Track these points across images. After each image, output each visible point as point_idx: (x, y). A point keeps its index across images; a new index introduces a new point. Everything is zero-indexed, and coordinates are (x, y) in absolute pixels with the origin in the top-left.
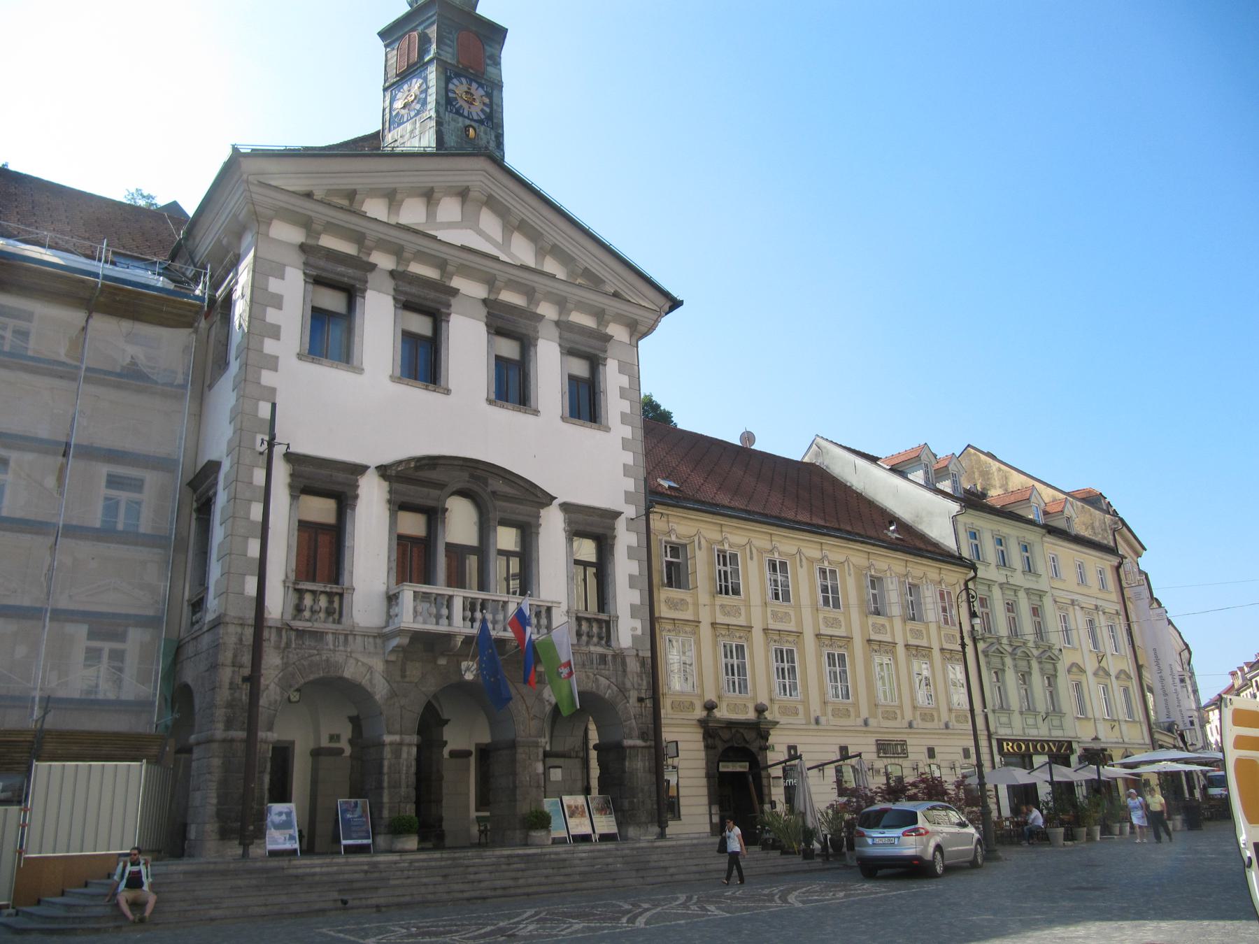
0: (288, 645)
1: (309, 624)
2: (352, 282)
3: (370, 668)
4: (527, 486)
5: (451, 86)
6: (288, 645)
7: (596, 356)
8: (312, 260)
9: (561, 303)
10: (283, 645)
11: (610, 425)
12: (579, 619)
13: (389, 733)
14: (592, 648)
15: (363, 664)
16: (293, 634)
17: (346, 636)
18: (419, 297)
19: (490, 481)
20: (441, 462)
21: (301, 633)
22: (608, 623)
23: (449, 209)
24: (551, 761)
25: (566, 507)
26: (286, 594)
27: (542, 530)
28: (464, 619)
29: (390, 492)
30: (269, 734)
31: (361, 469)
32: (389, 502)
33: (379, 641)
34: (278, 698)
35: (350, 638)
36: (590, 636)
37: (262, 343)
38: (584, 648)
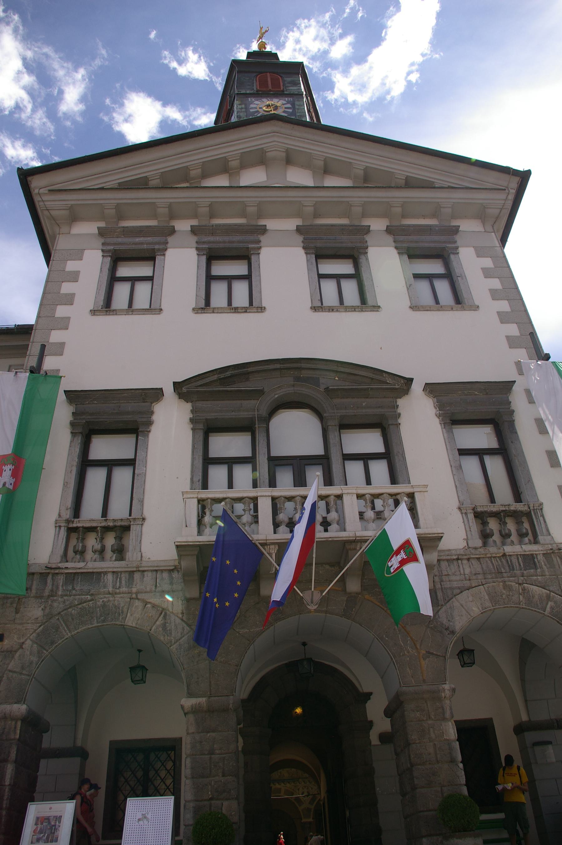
0: (53, 594)
1: (82, 564)
2: (151, 247)
3: (163, 612)
4: (370, 375)
5: (252, 106)
6: (53, 594)
7: (444, 249)
8: (109, 240)
9: (385, 212)
10: (47, 593)
11: (477, 303)
12: (481, 517)
13: (190, 695)
14: (508, 549)
15: (154, 606)
16: (61, 580)
17: (131, 573)
18: (224, 242)
19: (322, 381)
20: (250, 369)
21: (72, 577)
22: (528, 515)
23: (254, 177)
24: (531, 737)
25: (432, 389)
26: (57, 535)
27: (401, 421)
28: (276, 525)
29: (192, 411)
30: (16, 706)
31: (157, 394)
32: (192, 420)
33: (175, 575)
34: (35, 659)
35: (137, 576)
36: (505, 536)
37: (54, 310)
38: (492, 550)
